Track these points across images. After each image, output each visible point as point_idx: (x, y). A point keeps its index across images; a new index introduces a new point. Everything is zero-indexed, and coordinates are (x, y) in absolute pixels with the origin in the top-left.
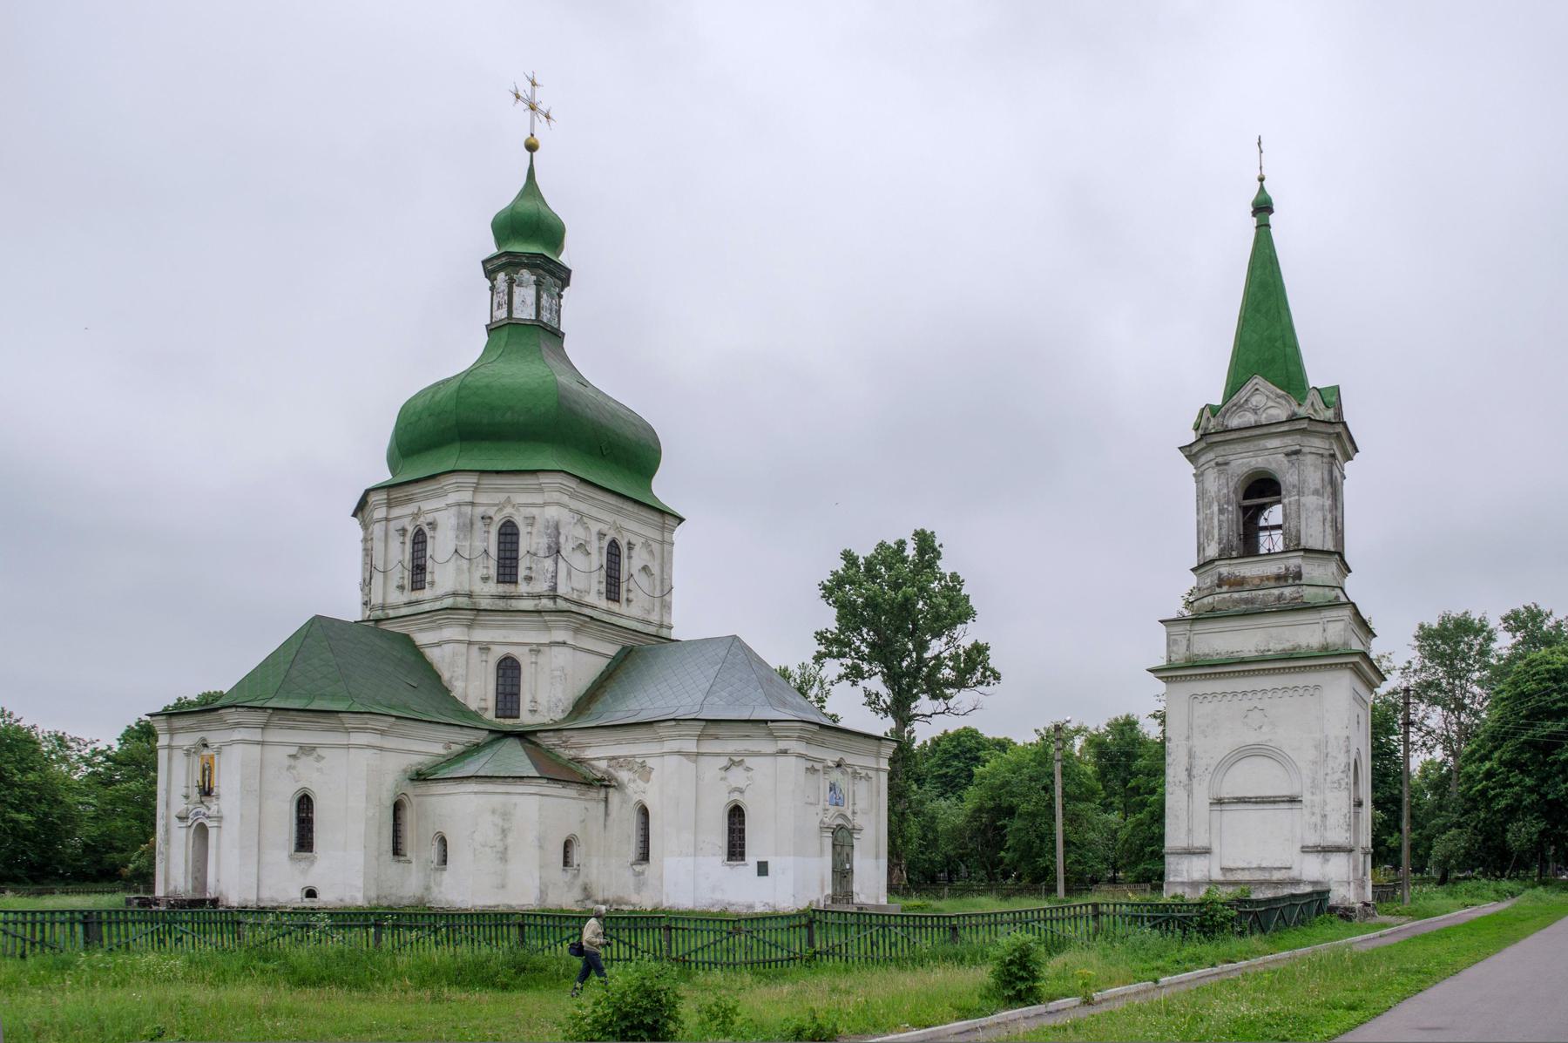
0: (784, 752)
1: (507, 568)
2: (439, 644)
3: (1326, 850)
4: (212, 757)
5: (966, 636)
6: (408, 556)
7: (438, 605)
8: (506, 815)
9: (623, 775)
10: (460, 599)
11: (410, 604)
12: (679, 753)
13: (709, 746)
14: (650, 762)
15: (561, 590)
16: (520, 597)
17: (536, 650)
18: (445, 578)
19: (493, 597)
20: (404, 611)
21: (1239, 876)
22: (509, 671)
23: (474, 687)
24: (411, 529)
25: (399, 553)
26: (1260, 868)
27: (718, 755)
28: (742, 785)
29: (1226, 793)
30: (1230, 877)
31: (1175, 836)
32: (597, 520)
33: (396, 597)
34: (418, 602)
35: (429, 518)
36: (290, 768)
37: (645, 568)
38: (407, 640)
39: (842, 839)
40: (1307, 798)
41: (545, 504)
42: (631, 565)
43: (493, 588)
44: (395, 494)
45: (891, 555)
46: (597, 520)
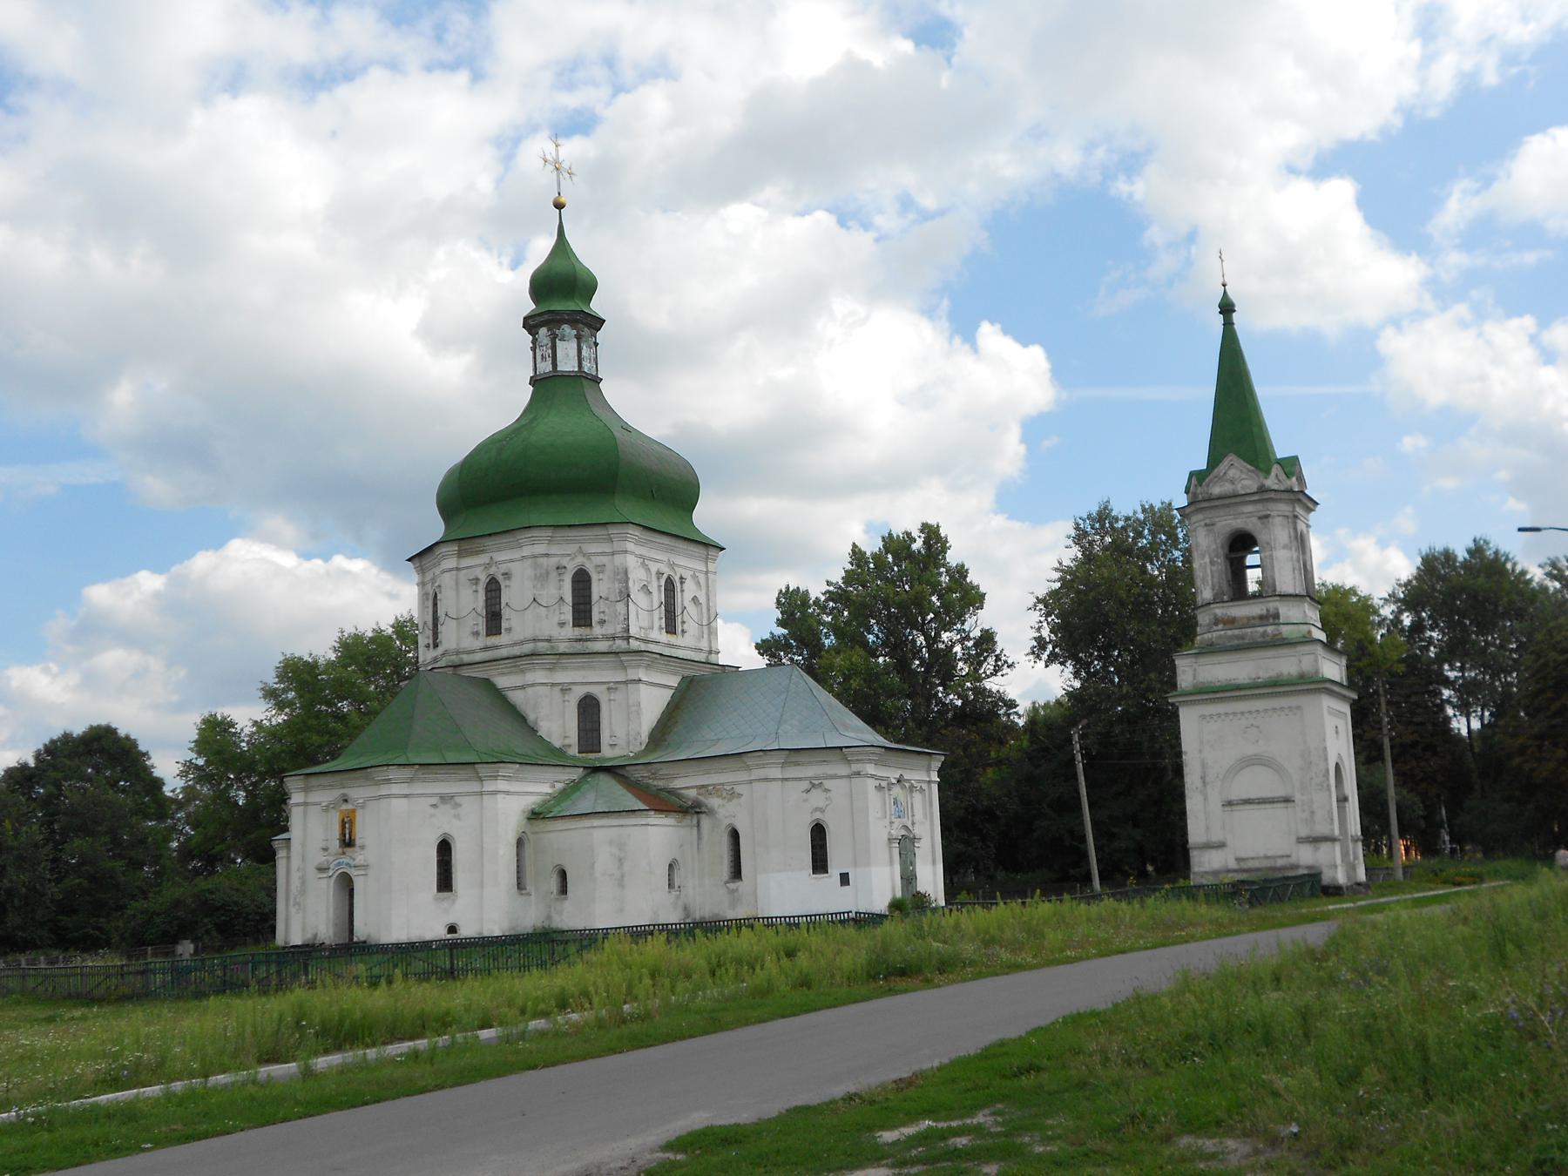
0: (858, 774)
1: (582, 615)
2: (523, 687)
3: (1316, 840)
4: (353, 811)
5: (975, 624)
7: (516, 651)
8: (621, 846)
9: (714, 802)
10: (540, 644)
11: (486, 649)
12: (766, 780)
13: (792, 772)
14: (738, 789)
15: (632, 632)
16: (595, 639)
17: (612, 687)
18: (521, 625)
19: (570, 640)
20: (479, 657)
21: (1250, 864)
22: (589, 709)
23: (559, 726)
24: (484, 579)
26: (1266, 857)
27: (800, 779)
28: (821, 804)
29: (1234, 797)
30: (1244, 865)
31: (1196, 832)
32: (657, 561)
34: (496, 647)
35: (503, 568)
36: (433, 816)
37: (695, 599)
38: (488, 684)
39: (906, 845)
40: (1298, 797)
41: (613, 554)
42: (684, 598)
43: (570, 631)
44: (465, 545)
45: (897, 546)
46: (657, 561)
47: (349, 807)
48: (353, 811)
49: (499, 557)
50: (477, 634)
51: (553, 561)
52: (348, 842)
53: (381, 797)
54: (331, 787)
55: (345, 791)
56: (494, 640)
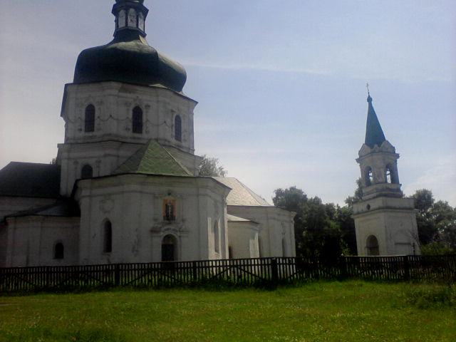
11: (134, 138)
20: (128, 140)
33: (123, 133)
34: (139, 138)
35: (145, 103)
43: (174, 141)
47: (170, 198)
48: (173, 201)
50: (129, 129)
51: (170, 108)
52: (169, 217)
55: (171, 188)
56: (137, 135)
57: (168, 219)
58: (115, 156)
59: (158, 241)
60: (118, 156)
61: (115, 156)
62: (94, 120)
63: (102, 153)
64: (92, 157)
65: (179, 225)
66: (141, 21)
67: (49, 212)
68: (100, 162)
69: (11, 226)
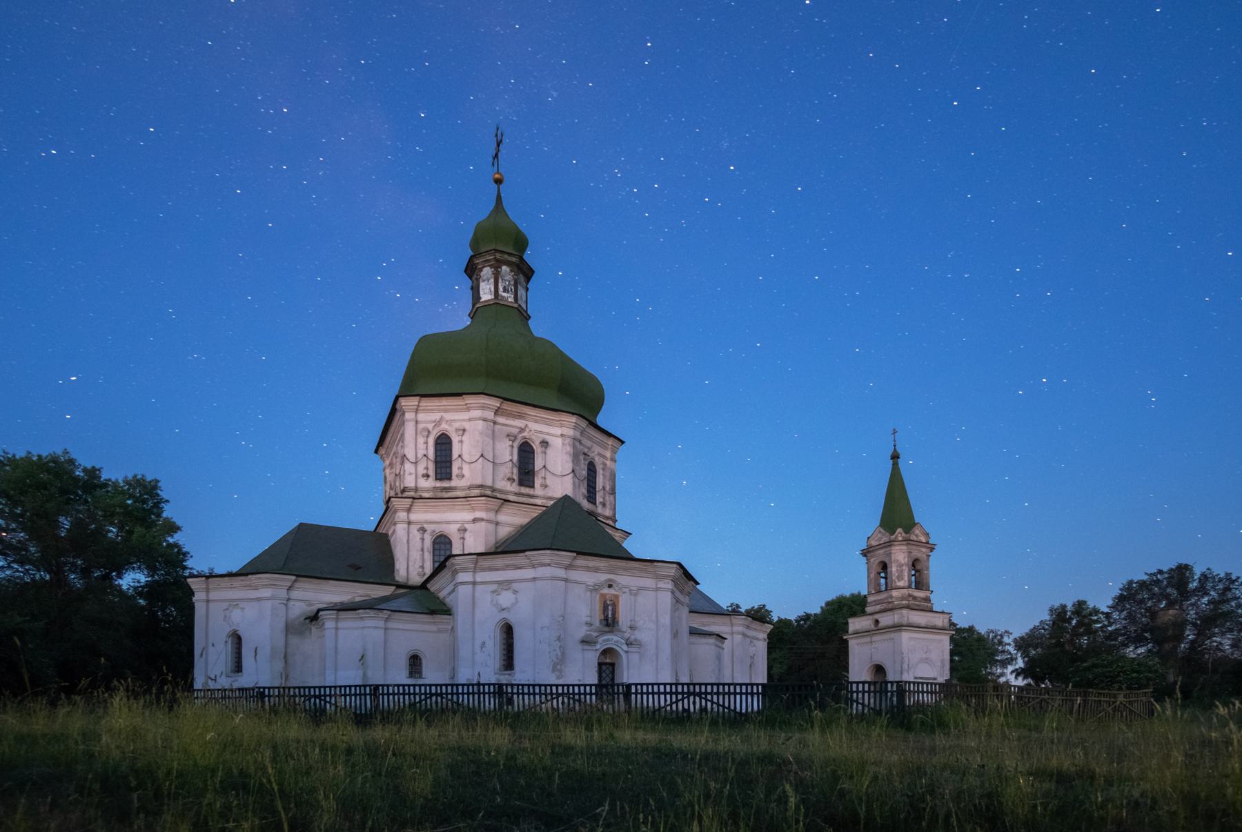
4: (617, 597)
6: (515, 458)
20: (511, 498)
25: (507, 453)
43: (586, 504)
47: (612, 591)
48: (617, 597)
49: (533, 426)
53: (657, 589)
54: (597, 570)
57: (608, 625)
58: (488, 521)
59: (592, 657)
60: (497, 524)
61: (488, 521)
62: (451, 462)
63: (468, 516)
64: (448, 523)
65: (627, 635)
66: (521, 292)
67: (394, 605)
68: (465, 530)
69: (329, 624)
